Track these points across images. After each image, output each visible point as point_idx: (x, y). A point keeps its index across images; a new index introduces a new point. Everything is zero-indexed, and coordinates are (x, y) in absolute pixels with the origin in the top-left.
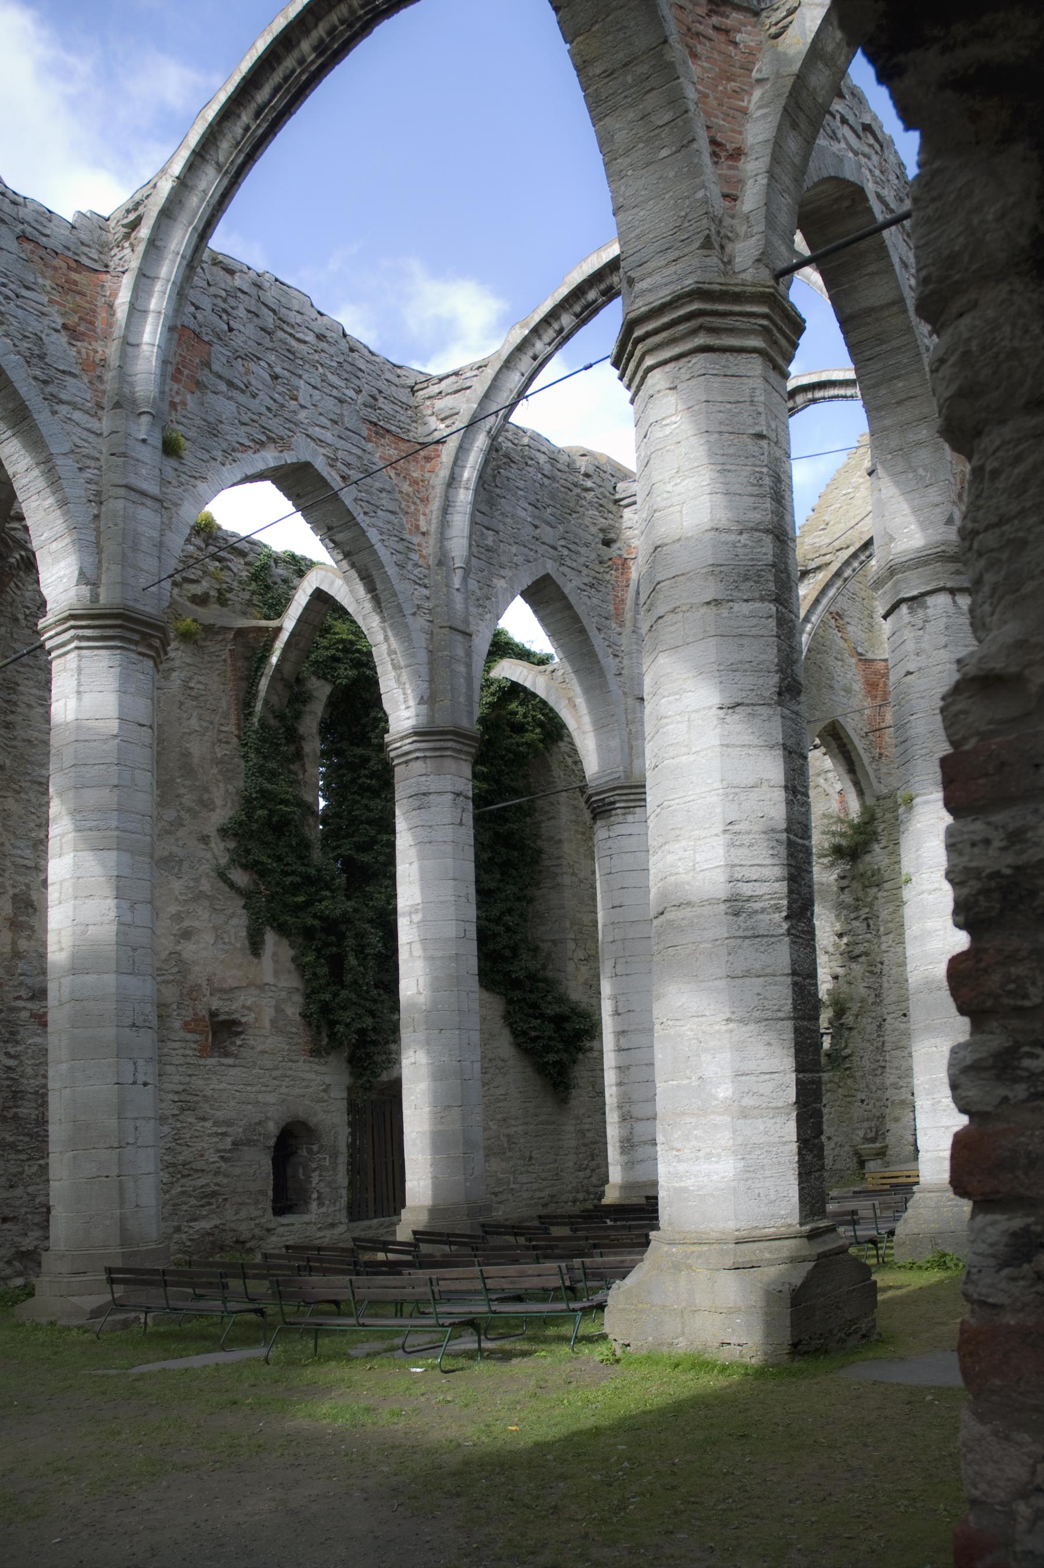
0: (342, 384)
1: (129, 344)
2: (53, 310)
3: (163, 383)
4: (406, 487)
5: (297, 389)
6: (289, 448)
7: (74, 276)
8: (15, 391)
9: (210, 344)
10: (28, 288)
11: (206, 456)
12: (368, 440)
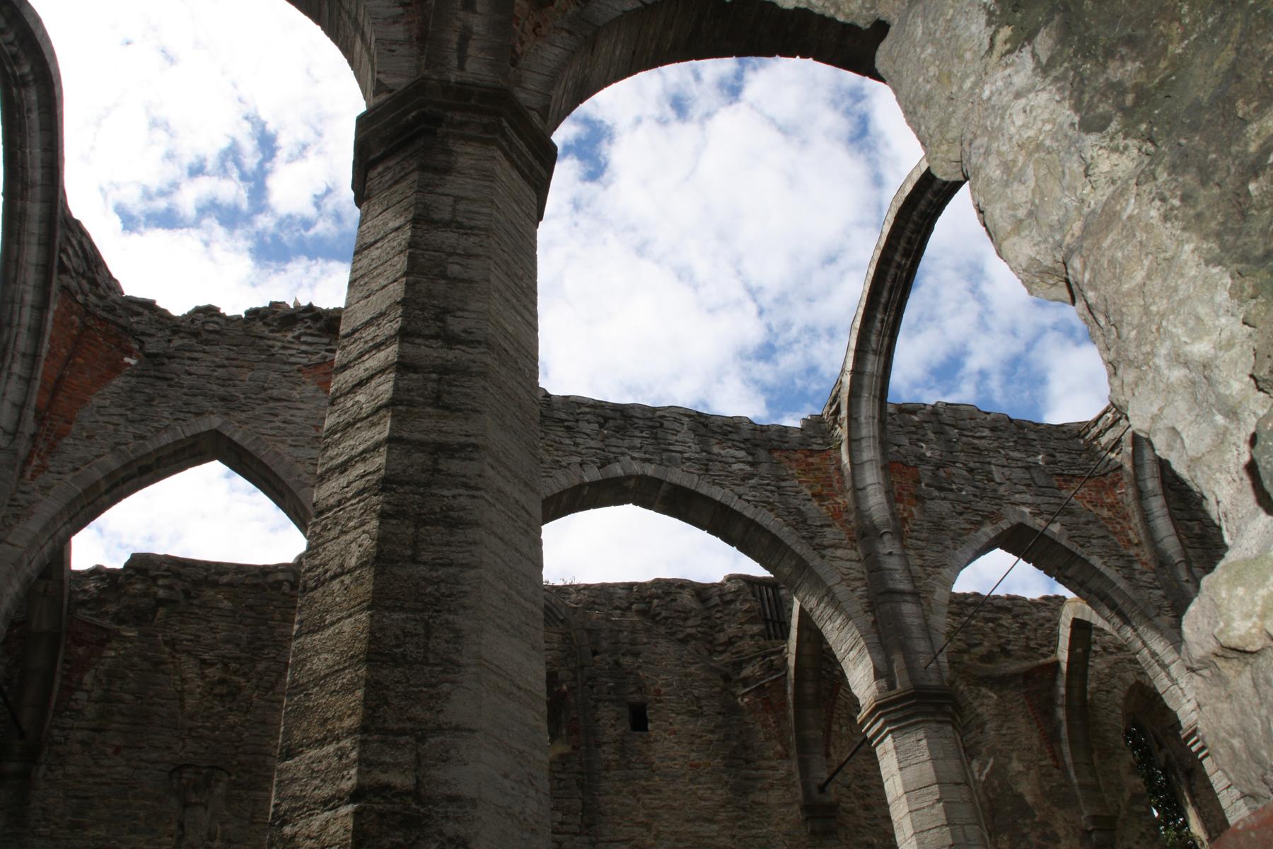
0: (1023, 455)
1: (858, 490)
2: (803, 487)
3: (891, 507)
4: (1105, 513)
5: (990, 472)
6: (1000, 518)
7: (811, 460)
8: (793, 552)
9: (916, 467)
10: (784, 480)
11: (941, 548)
12: (1060, 488)
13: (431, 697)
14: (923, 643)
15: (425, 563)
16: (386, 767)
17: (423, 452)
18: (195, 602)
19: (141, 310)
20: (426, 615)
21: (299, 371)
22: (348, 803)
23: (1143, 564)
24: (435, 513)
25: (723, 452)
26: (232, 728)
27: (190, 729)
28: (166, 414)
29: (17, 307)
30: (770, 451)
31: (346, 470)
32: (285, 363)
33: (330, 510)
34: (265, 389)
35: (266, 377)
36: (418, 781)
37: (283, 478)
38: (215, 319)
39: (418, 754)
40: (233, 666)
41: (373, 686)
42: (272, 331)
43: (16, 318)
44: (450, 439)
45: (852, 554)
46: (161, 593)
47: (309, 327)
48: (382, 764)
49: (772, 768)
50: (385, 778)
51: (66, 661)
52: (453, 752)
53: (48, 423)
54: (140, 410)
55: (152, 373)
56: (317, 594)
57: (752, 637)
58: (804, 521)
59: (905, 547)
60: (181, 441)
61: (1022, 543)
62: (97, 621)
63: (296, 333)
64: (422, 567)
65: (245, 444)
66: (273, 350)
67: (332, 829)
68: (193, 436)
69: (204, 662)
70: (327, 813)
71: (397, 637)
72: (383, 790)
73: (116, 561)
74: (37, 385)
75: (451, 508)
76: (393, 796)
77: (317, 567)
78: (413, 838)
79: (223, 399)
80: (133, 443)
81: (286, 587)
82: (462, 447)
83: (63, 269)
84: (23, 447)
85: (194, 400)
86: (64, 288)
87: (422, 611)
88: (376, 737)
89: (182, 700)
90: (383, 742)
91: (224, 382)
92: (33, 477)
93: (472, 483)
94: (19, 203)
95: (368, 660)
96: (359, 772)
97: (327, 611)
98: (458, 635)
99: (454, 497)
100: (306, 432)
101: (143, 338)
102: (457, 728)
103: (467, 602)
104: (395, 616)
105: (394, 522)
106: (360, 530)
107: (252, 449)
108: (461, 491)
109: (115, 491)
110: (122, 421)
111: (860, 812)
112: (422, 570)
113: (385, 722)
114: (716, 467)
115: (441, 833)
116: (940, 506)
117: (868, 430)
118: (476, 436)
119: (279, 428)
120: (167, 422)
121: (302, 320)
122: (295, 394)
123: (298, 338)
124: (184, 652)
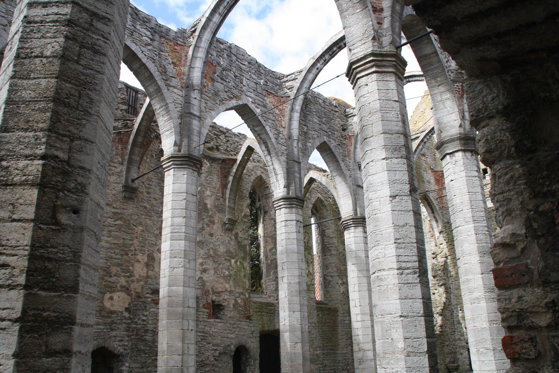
1: (191, 67)
3: (202, 79)
11: (214, 103)
13: (78, 124)
14: (197, 138)
15: (82, 65)
16: (57, 149)
17: (87, 14)
20: (80, 88)
22: (39, 159)
23: (283, 135)
24: (89, 44)
25: (141, 30)
30: (161, 37)
31: (46, 7)
36: (69, 158)
39: (70, 147)
41: (55, 113)
44: (99, 12)
45: (180, 93)
48: (55, 147)
49: (115, 167)
50: (56, 153)
52: (84, 149)
56: (27, 61)
57: (121, 110)
58: (165, 72)
59: (201, 98)
61: (244, 112)
64: (81, 67)
67: (30, 168)
70: (27, 161)
71: (67, 94)
72: (55, 158)
75: (95, 44)
76: (59, 161)
77: (27, 48)
78: (65, 180)
82: (104, 18)
88: (54, 135)
90: (57, 138)
93: (106, 36)
95: (54, 101)
96: (46, 148)
97: (32, 72)
98: (91, 101)
99: (97, 39)
102: (86, 140)
103: (97, 88)
104: (67, 85)
105: (71, 42)
106: (54, 40)
108: (101, 38)
111: (145, 194)
113: (58, 129)
114: (136, 35)
115: (76, 180)
116: (219, 86)
117: (204, 44)
118: (110, 15)
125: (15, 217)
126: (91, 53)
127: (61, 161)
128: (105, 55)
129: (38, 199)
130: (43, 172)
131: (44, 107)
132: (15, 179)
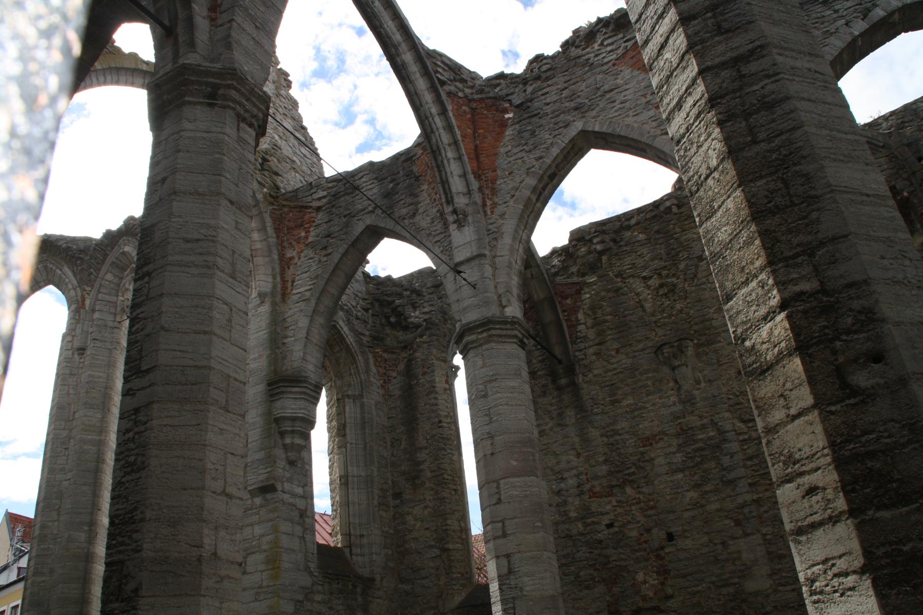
13: (807, 225)
15: (763, 141)
16: (795, 282)
17: (727, 68)
18: (622, 243)
19: (498, 81)
20: (780, 174)
21: (614, 65)
22: (780, 313)
24: (754, 105)
26: (681, 311)
27: (655, 322)
28: (547, 136)
29: (430, 119)
31: (681, 107)
32: (602, 65)
33: (683, 137)
34: (599, 89)
35: (595, 80)
36: (821, 283)
37: (639, 139)
38: (544, 61)
39: (814, 266)
40: (664, 273)
41: (764, 234)
42: (583, 49)
43: (434, 126)
44: (741, 51)
46: (599, 247)
47: (605, 33)
48: (792, 280)
50: (797, 289)
51: (564, 311)
52: (838, 255)
53: (483, 177)
54: (531, 142)
55: (525, 116)
56: (701, 193)
60: (564, 148)
62: (569, 280)
63: (599, 42)
64: (763, 144)
65: (604, 130)
66: (591, 61)
67: (776, 332)
68: (570, 141)
69: (645, 278)
70: (769, 325)
71: (766, 197)
72: (799, 296)
73: (563, 240)
74: (465, 158)
75: (764, 96)
77: (693, 176)
79: (576, 109)
80: (537, 164)
81: (675, 209)
82: (752, 52)
83: (443, 83)
84: (477, 197)
85: (559, 119)
86: (449, 94)
87: (776, 172)
88: (780, 265)
89: (642, 306)
91: (571, 98)
92: (492, 212)
93: (771, 72)
94: (398, 59)
95: (754, 219)
96: (779, 291)
97: (713, 201)
98: (807, 178)
99: (763, 88)
100: (639, 102)
101: (509, 98)
102: (834, 239)
104: (759, 184)
105: (730, 124)
106: (710, 140)
107: (610, 131)
108: (766, 81)
109: (542, 198)
110: (523, 154)
112: (764, 146)
113: (782, 253)
115: (851, 310)
118: (758, 39)
119: (620, 108)
120: (550, 141)
121: (598, 31)
122: (619, 81)
123: (602, 44)
124: (629, 277)
125: (793, 411)
126: (766, 113)
127: (811, 295)
128: (788, 98)
129: (806, 370)
130: (792, 328)
131: (749, 237)
132: (768, 358)
